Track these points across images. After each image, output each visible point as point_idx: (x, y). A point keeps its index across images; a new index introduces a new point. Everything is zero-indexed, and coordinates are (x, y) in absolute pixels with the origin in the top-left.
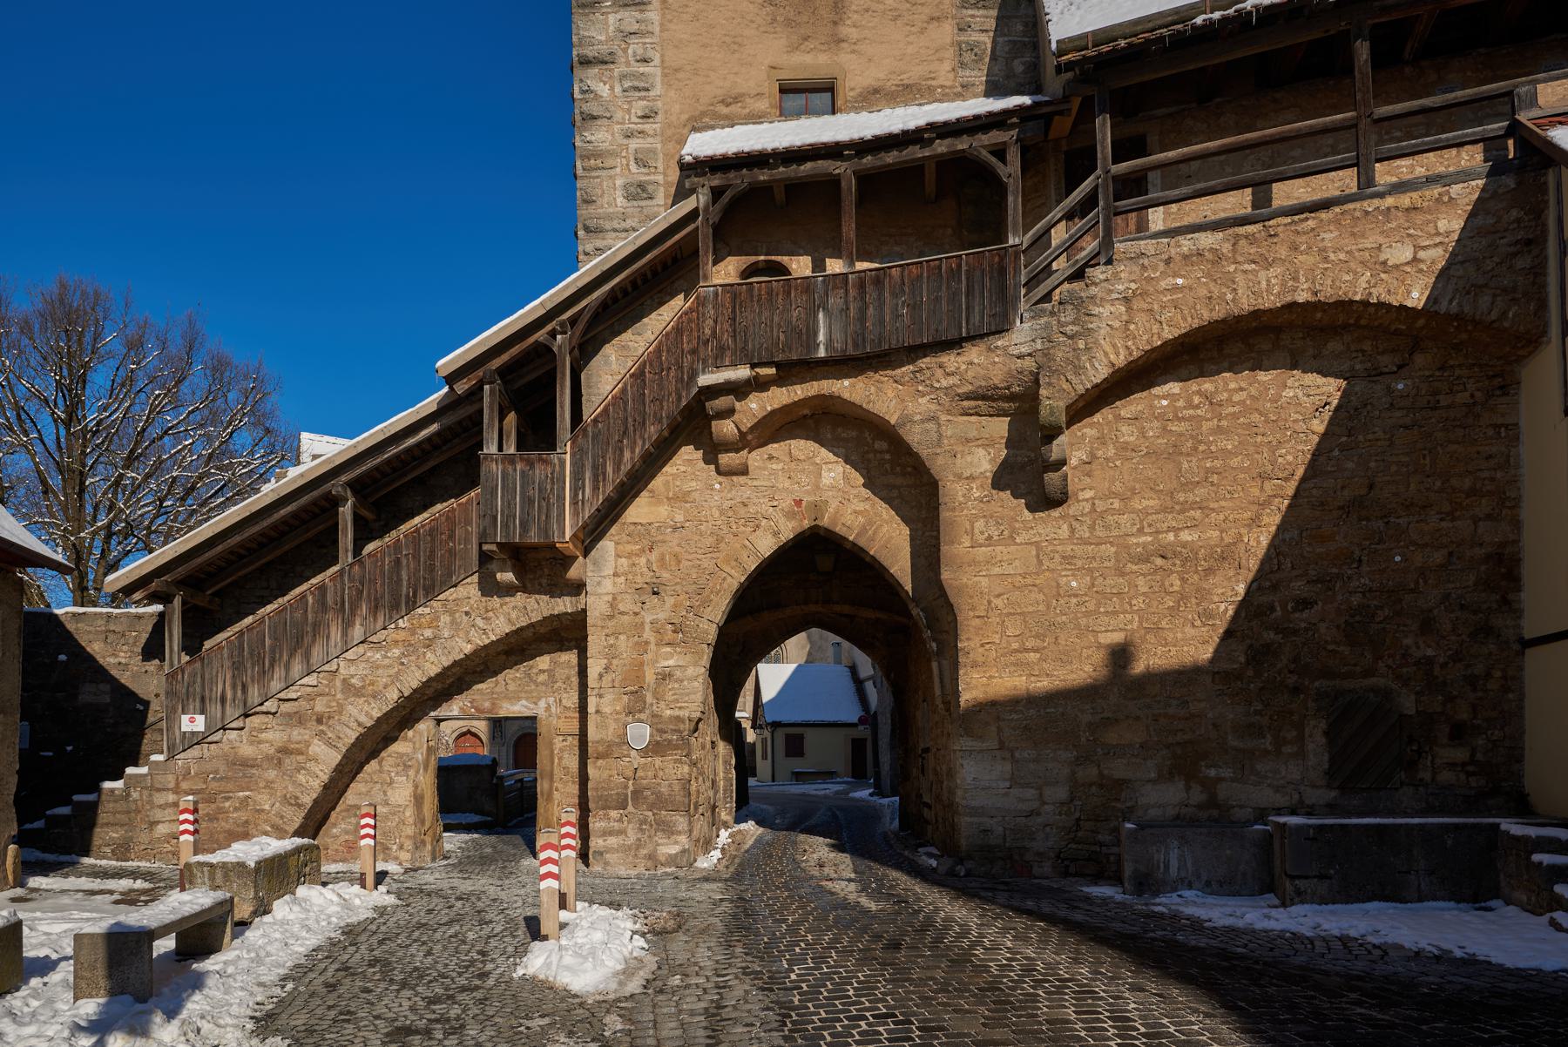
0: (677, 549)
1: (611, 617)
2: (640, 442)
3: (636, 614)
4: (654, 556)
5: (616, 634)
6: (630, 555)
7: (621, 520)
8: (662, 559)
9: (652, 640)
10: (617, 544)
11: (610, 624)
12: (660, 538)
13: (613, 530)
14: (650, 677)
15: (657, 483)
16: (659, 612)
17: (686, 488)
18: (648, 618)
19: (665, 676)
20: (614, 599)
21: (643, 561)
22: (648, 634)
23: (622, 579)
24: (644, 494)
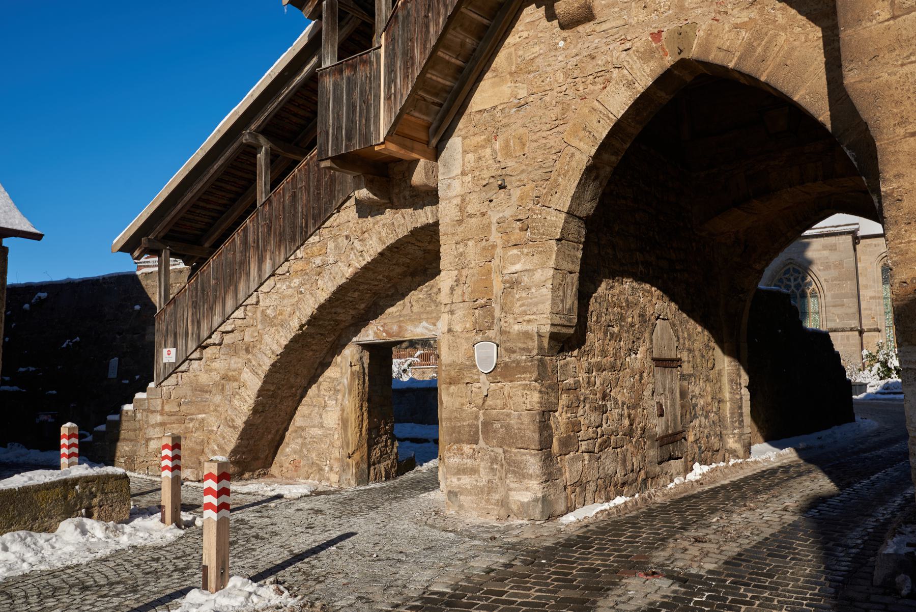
0: (521, 131)
1: (460, 222)
2: (443, 11)
3: (483, 214)
4: (497, 145)
5: (465, 241)
6: (477, 148)
7: (468, 111)
8: (507, 146)
9: (499, 242)
10: (464, 138)
11: (460, 229)
12: (504, 121)
13: (460, 125)
14: (497, 287)
15: (501, 59)
16: (506, 208)
17: (528, 56)
18: (494, 217)
19: (513, 284)
20: (463, 200)
21: (488, 152)
22: (495, 237)
23: (469, 178)
24: (489, 75)
